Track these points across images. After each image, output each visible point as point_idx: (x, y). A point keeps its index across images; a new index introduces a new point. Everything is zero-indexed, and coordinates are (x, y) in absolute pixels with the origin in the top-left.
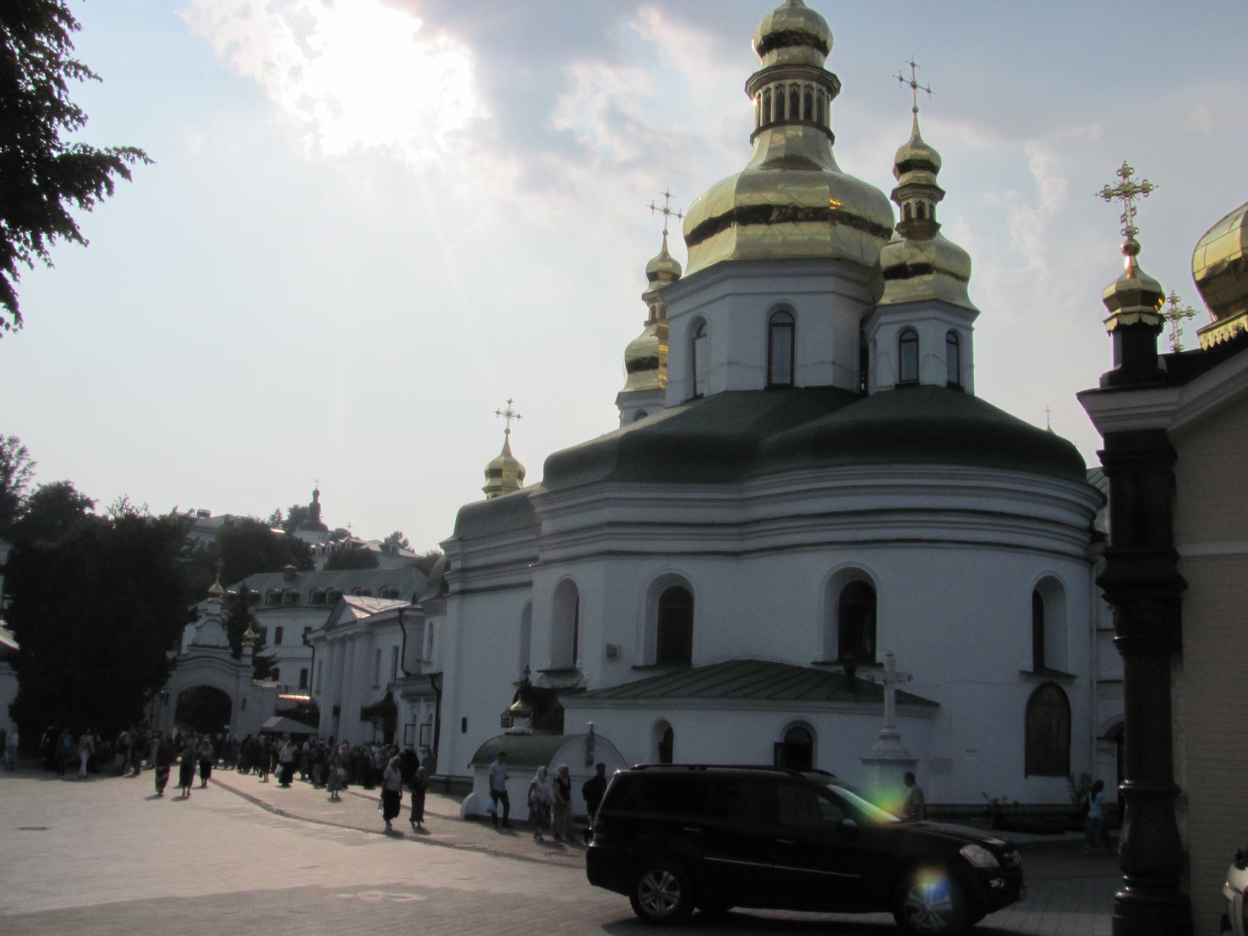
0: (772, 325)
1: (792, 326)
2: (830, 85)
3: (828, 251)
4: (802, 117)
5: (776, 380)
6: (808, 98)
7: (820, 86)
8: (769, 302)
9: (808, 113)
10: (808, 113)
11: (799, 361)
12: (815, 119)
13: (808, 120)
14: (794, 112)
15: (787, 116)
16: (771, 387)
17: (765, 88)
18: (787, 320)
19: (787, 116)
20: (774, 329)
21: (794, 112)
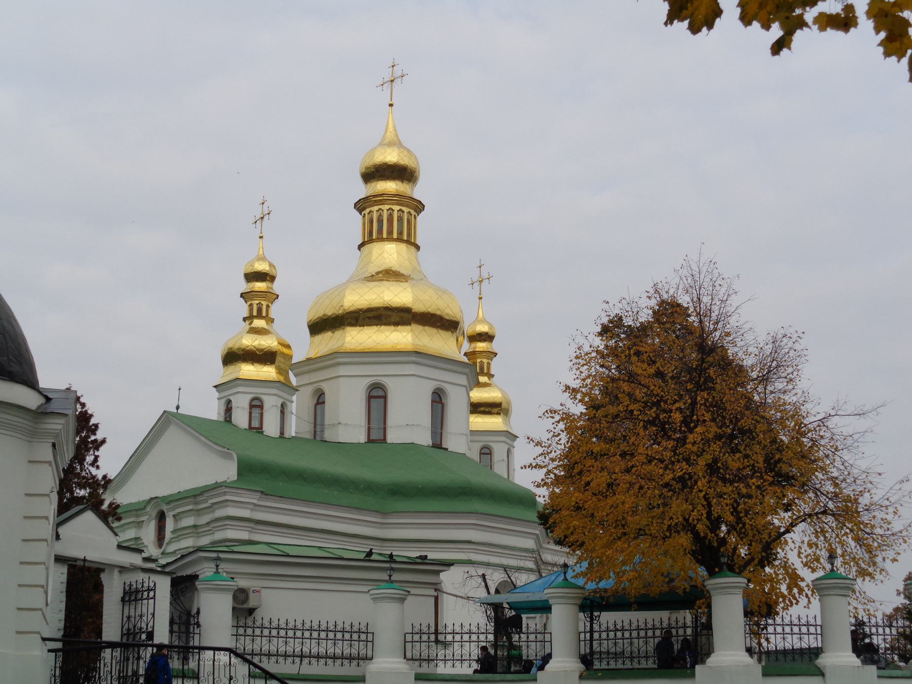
0: (370, 398)
1: (385, 398)
2: (419, 207)
3: (410, 348)
4: (395, 236)
5: (372, 438)
6: (400, 219)
7: (409, 210)
8: (367, 381)
9: (400, 233)
10: (400, 233)
11: (390, 422)
12: (405, 238)
13: (400, 240)
14: (390, 232)
15: (385, 236)
16: (370, 441)
17: (368, 210)
18: (381, 393)
19: (385, 236)
20: (372, 400)
21: (390, 232)
